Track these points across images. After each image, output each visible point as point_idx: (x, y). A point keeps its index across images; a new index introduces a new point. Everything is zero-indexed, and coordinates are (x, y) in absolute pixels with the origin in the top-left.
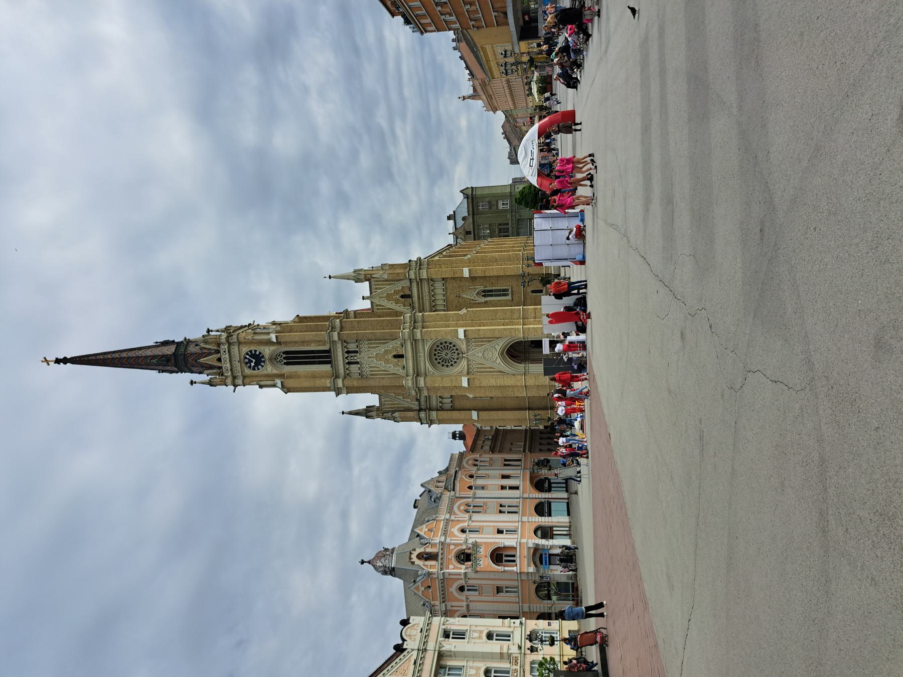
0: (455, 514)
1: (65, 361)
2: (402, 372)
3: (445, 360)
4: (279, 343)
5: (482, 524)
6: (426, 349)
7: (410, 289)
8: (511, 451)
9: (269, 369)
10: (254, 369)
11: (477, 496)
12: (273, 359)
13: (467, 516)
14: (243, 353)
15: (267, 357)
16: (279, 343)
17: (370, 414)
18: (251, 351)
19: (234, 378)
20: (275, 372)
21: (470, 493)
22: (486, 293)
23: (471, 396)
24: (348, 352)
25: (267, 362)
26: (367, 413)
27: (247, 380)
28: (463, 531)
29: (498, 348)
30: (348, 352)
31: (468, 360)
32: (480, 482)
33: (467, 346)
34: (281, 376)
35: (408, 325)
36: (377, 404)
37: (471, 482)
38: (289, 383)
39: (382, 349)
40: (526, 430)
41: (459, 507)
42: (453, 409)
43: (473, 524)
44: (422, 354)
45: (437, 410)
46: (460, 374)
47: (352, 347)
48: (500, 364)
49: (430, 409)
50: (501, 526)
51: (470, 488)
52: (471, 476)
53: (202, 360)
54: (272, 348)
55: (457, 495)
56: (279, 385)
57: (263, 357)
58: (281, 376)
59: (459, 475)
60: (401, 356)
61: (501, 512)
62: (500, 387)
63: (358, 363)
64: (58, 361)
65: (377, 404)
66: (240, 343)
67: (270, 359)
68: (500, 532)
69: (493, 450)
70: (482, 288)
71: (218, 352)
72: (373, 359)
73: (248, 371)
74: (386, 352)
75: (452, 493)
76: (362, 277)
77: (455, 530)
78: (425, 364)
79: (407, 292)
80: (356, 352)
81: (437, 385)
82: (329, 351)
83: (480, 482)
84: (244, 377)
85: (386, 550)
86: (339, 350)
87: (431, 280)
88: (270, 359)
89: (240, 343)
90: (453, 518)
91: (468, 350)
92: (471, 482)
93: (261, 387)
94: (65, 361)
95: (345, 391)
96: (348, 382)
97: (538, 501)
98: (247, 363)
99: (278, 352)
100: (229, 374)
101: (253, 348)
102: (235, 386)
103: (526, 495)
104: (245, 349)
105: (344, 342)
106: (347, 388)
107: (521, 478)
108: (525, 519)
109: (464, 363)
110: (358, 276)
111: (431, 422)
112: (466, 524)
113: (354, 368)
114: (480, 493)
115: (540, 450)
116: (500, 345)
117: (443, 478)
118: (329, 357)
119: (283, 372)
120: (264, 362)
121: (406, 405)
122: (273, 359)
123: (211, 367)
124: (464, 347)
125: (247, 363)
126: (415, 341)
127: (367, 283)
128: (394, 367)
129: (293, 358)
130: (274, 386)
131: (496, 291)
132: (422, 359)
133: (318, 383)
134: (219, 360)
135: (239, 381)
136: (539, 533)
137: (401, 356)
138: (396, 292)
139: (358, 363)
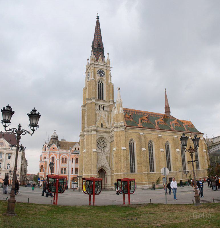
9: (98, 77)
14: (103, 70)
24: (104, 107)
25: (100, 77)
30: (104, 107)
33: (106, 153)
39: (105, 120)
44: (103, 135)
60: (102, 127)
74: (104, 122)
82: (103, 100)
88: (101, 79)
91: (105, 153)
99: (103, 81)
100: (96, 63)
109: (100, 151)
118: (101, 99)
122: (100, 80)
132: (101, 135)
137: (102, 127)
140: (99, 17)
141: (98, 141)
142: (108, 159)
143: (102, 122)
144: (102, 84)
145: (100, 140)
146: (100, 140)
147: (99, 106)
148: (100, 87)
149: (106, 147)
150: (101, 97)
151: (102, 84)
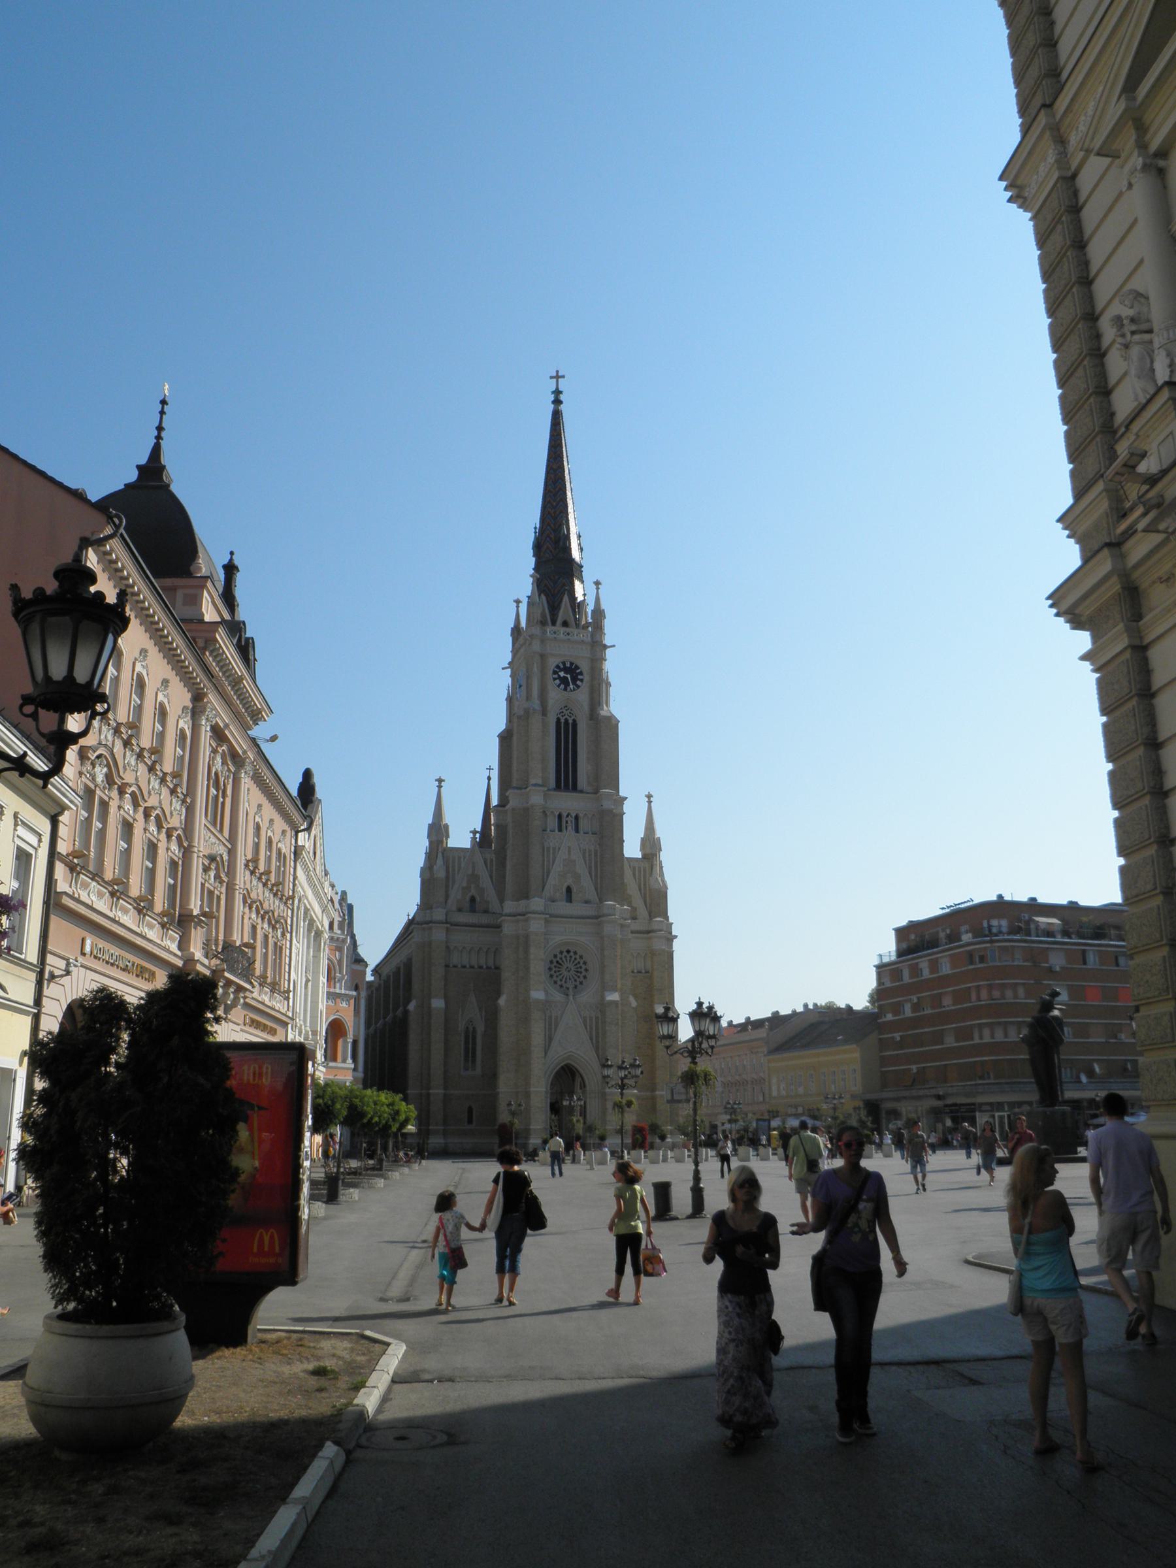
1: (557, 402)
10: (555, 672)
18: (581, 673)
20: (550, 702)
30: (577, 818)
39: (581, 869)
48: (559, 1054)
64: (557, 392)
80: (577, 831)
82: (575, 788)
94: (557, 402)
98: (564, 663)
101: (586, 677)
109: (558, 997)
118: (567, 789)
125: (564, 663)
129: (566, 733)
143: (569, 881)
144: (570, 721)
147: (560, 816)
148: (566, 733)
151: (570, 721)
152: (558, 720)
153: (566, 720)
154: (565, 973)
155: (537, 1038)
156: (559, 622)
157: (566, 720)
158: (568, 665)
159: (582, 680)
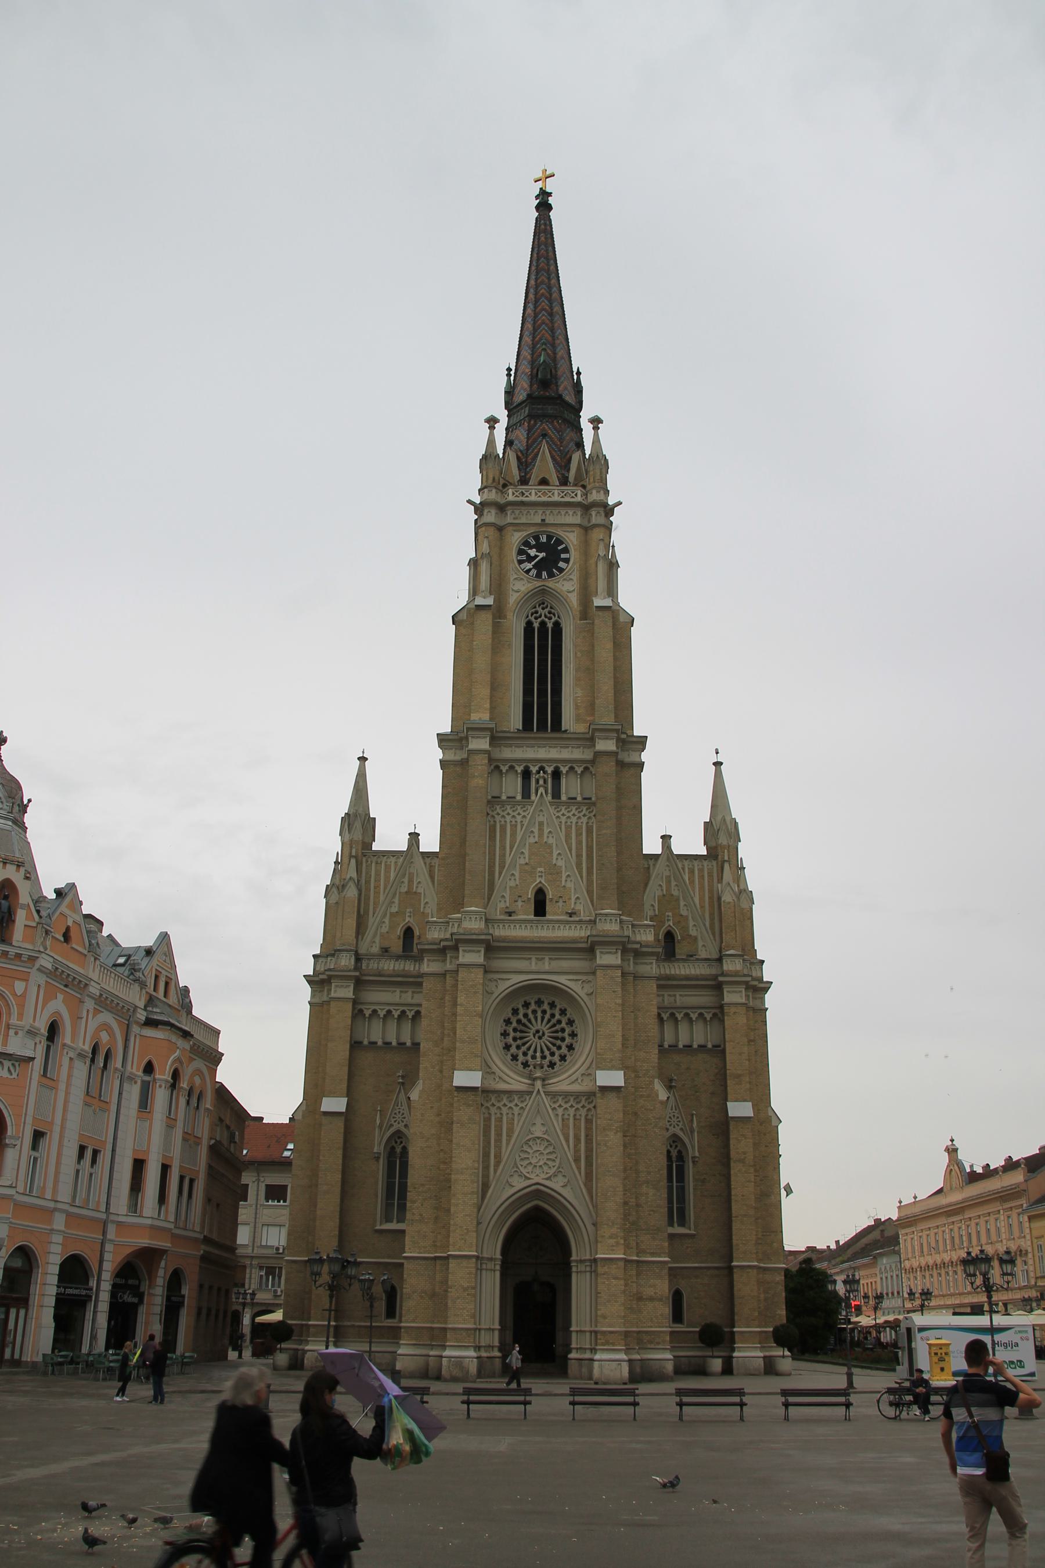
0: (96, 1012)
2: (500, 905)
3: (522, 1028)
4: (586, 610)
5: (62, 1086)
6: (562, 979)
7: (691, 957)
8: (208, 1200)
9: (520, 585)
10: (521, 552)
11: (126, 1085)
12: (542, 598)
13: (88, 1048)
14: (561, 533)
15: (551, 584)
16: (586, 610)
17: (358, 824)
18: (566, 550)
19: (501, 508)
20: (513, 599)
21: (136, 1069)
22: (676, 1162)
23: (414, 1095)
24: (556, 775)
25: (538, 583)
26: (358, 823)
27: (491, 532)
28: (53, 1030)
29: (557, 1184)
30: (556, 775)
31: (522, 1094)
32: (160, 1096)
33: (566, 1095)
34: (498, 611)
35: (628, 932)
36: (376, 847)
37: (163, 1075)
38: (484, 622)
39: (563, 860)
40: (232, 1248)
41: (105, 1027)
42: (355, 1045)
43: (66, 1062)
44: (546, 966)
45: (355, 1002)
46: (488, 1071)
47: (571, 787)
48: (510, 1186)
49: (359, 983)
50: (50, 1145)
51: (149, 1068)
52: (176, 1075)
53: (545, 448)
54: (574, 599)
55: (135, 1029)
56: (480, 601)
57: (551, 575)
58: (498, 611)
59: (181, 1043)
60: (540, 907)
61: (82, 1149)
62: (444, 1184)
63: (526, 794)
65: (376, 847)
66: (586, 529)
67: (543, 591)
68: (38, 1135)
69: (215, 1150)
70: (693, 1150)
71: (564, 482)
72: (545, 838)
73: (515, 538)
74: (554, 872)
75: (142, 1016)
76: (723, 840)
77: (58, 1005)
78: (518, 973)
79: (681, 950)
80: (556, 794)
81: (461, 999)
82: (557, 725)
83: (160, 1096)
84: (500, 529)
85: (24, 809)
86: (566, 754)
87: (719, 1013)
88: (543, 591)
89: (586, 529)
90: (89, 1004)
91: (553, 1096)
92: (163, 1075)
93: (474, 563)
95: (451, 756)
96: (480, 764)
97: (94, 1267)
98: (537, 538)
101: (574, 555)
102: (479, 509)
103: (111, 1230)
104: (572, 539)
105: (588, 768)
106: (464, 763)
107: (145, 1221)
108: (59, 1222)
109: (514, 1081)
110: (722, 833)
111: (318, 982)
112: (68, 1041)
113: (512, 786)
114: (133, 1093)
115: (201, 1286)
116: (567, 1189)
117: (173, 1000)
118: (542, 727)
119: (509, 615)
120: (539, 576)
121: (372, 921)
122: (542, 598)
123: (525, 463)
124: (565, 1081)
125: (537, 538)
126: (590, 949)
127: (703, 851)
128: (513, 886)
129: (543, 646)
130: (474, 591)
131: (682, 1190)
132: (534, 967)
133: (483, 692)
134: (544, 482)
135: (490, 516)
136: (18, 1263)
137: (540, 907)
138: (681, 920)
139: (526, 794)
140: (550, 194)
141: (515, 1012)
142: (577, 1139)
144: (550, 625)
145: (526, 1005)
146: (526, 1005)
148: (543, 646)
149: (563, 1058)
150: (542, 712)
151: (550, 625)
152: (529, 628)
153: (543, 624)
154: (534, 1041)
155: (465, 1160)
156: (534, 478)
157: (543, 624)
158: (544, 539)
159: (567, 561)
